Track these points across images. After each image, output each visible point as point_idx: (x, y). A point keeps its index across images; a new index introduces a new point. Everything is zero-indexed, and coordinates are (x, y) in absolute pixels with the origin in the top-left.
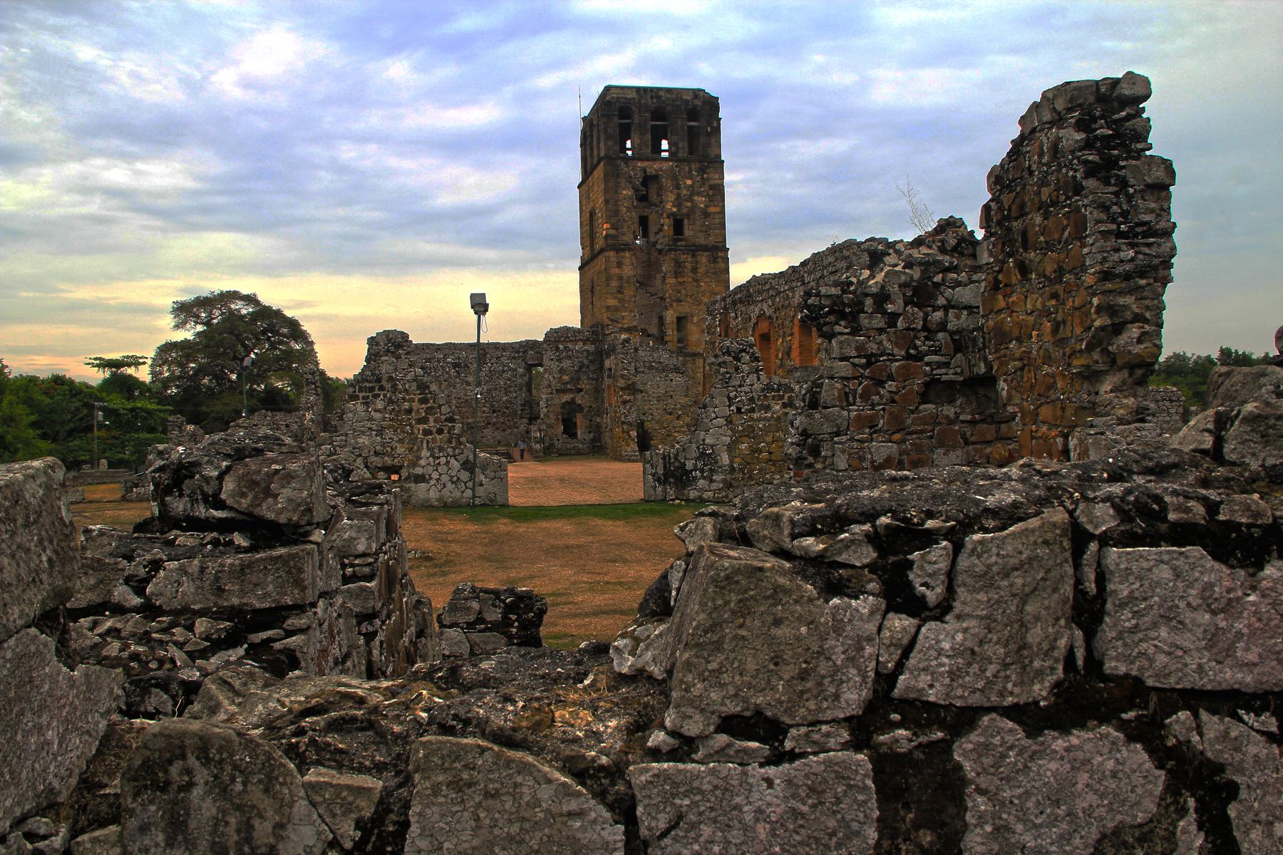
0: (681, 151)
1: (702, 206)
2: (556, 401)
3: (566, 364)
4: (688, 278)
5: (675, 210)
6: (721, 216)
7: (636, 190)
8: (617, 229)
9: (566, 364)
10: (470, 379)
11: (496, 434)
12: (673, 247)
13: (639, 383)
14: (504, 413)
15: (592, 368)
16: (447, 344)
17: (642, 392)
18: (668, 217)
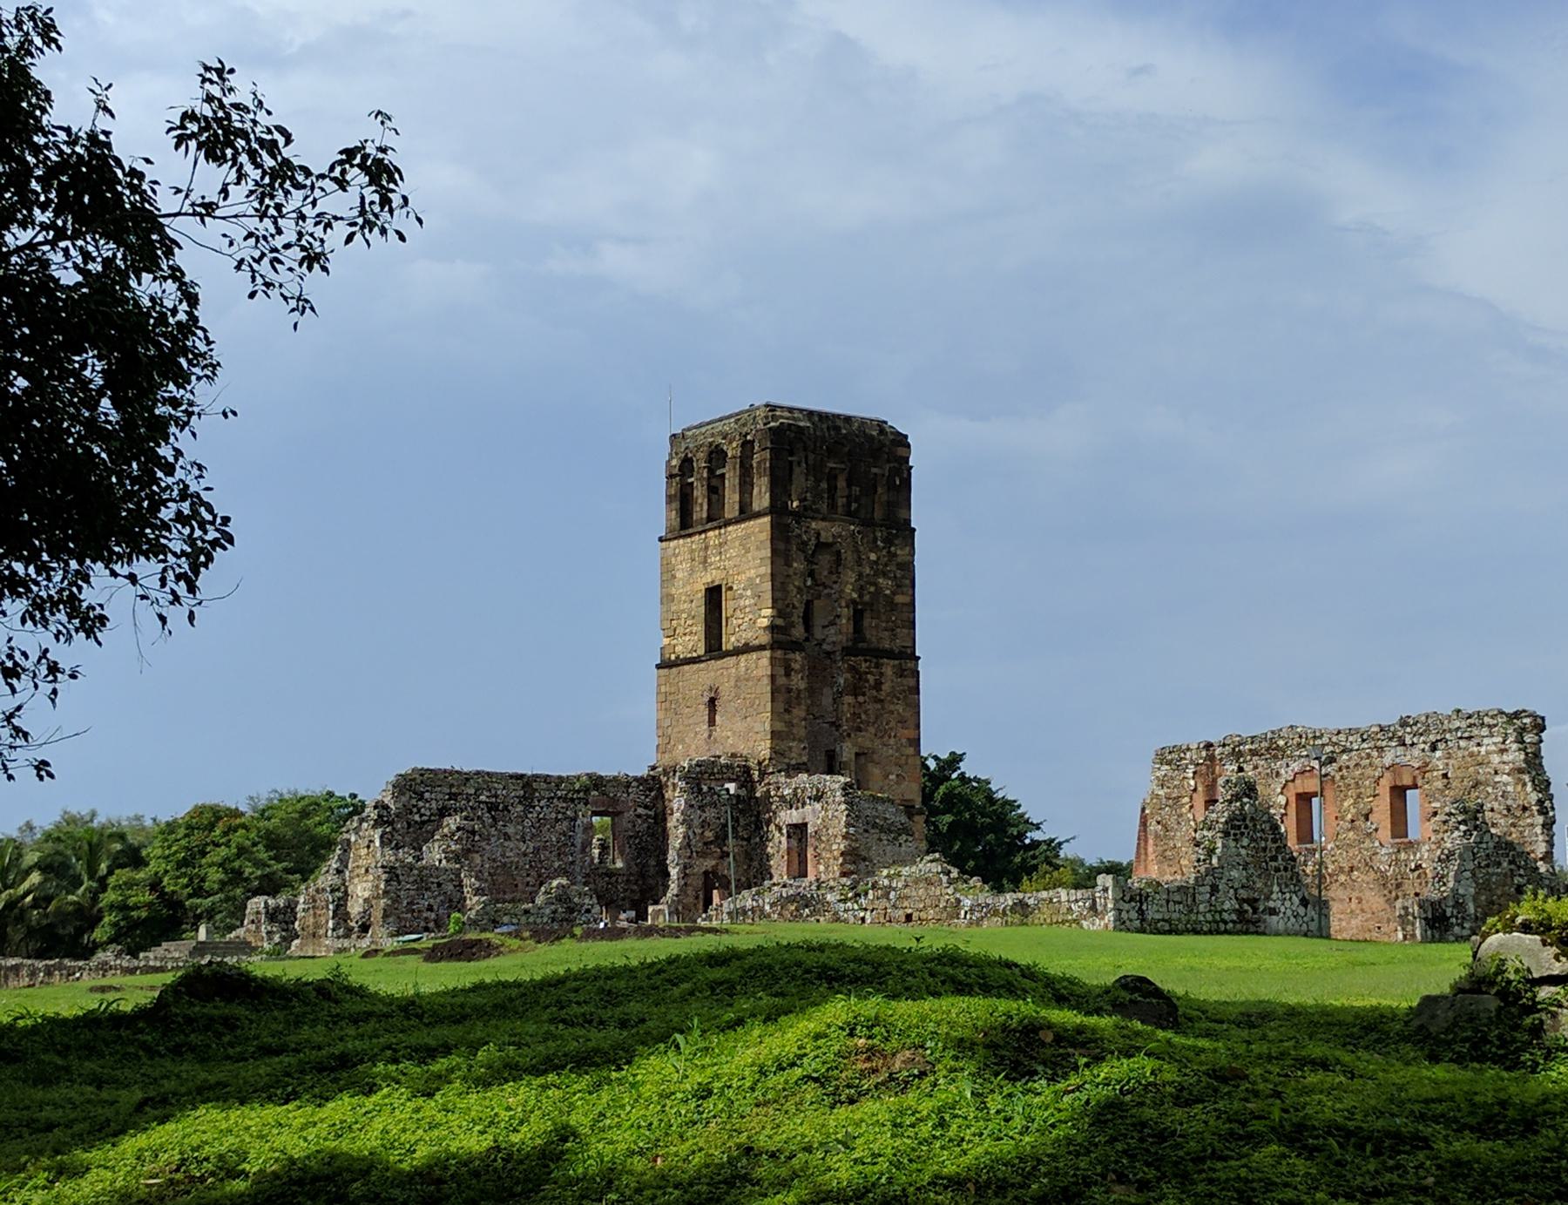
1: (888, 592)
3: (710, 814)
5: (855, 595)
10: (510, 830)
17: (864, 859)
18: (847, 606)
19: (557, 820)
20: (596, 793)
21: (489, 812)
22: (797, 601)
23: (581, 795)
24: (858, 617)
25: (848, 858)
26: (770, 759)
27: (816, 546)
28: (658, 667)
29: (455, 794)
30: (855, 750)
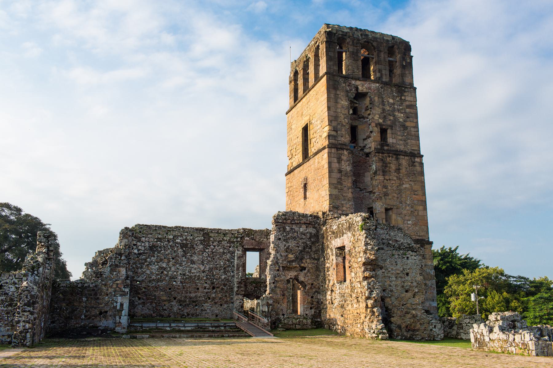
0: (384, 77)
1: (401, 120)
2: (283, 278)
3: (292, 244)
4: (393, 176)
5: (381, 121)
6: (416, 130)
7: (351, 102)
8: (337, 132)
9: (292, 244)
10: (195, 258)
12: (379, 151)
13: (380, 259)
14: (222, 289)
15: (314, 249)
16: (176, 227)
17: (381, 268)
18: (376, 126)
19: (224, 253)
21: (182, 248)
23: (239, 239)
24: (383, 132)
25: (369, 267)
26: (330, 211)
27: (356, 94)
28: (286, 175)
29: (160, 239)
30: (385, 206)
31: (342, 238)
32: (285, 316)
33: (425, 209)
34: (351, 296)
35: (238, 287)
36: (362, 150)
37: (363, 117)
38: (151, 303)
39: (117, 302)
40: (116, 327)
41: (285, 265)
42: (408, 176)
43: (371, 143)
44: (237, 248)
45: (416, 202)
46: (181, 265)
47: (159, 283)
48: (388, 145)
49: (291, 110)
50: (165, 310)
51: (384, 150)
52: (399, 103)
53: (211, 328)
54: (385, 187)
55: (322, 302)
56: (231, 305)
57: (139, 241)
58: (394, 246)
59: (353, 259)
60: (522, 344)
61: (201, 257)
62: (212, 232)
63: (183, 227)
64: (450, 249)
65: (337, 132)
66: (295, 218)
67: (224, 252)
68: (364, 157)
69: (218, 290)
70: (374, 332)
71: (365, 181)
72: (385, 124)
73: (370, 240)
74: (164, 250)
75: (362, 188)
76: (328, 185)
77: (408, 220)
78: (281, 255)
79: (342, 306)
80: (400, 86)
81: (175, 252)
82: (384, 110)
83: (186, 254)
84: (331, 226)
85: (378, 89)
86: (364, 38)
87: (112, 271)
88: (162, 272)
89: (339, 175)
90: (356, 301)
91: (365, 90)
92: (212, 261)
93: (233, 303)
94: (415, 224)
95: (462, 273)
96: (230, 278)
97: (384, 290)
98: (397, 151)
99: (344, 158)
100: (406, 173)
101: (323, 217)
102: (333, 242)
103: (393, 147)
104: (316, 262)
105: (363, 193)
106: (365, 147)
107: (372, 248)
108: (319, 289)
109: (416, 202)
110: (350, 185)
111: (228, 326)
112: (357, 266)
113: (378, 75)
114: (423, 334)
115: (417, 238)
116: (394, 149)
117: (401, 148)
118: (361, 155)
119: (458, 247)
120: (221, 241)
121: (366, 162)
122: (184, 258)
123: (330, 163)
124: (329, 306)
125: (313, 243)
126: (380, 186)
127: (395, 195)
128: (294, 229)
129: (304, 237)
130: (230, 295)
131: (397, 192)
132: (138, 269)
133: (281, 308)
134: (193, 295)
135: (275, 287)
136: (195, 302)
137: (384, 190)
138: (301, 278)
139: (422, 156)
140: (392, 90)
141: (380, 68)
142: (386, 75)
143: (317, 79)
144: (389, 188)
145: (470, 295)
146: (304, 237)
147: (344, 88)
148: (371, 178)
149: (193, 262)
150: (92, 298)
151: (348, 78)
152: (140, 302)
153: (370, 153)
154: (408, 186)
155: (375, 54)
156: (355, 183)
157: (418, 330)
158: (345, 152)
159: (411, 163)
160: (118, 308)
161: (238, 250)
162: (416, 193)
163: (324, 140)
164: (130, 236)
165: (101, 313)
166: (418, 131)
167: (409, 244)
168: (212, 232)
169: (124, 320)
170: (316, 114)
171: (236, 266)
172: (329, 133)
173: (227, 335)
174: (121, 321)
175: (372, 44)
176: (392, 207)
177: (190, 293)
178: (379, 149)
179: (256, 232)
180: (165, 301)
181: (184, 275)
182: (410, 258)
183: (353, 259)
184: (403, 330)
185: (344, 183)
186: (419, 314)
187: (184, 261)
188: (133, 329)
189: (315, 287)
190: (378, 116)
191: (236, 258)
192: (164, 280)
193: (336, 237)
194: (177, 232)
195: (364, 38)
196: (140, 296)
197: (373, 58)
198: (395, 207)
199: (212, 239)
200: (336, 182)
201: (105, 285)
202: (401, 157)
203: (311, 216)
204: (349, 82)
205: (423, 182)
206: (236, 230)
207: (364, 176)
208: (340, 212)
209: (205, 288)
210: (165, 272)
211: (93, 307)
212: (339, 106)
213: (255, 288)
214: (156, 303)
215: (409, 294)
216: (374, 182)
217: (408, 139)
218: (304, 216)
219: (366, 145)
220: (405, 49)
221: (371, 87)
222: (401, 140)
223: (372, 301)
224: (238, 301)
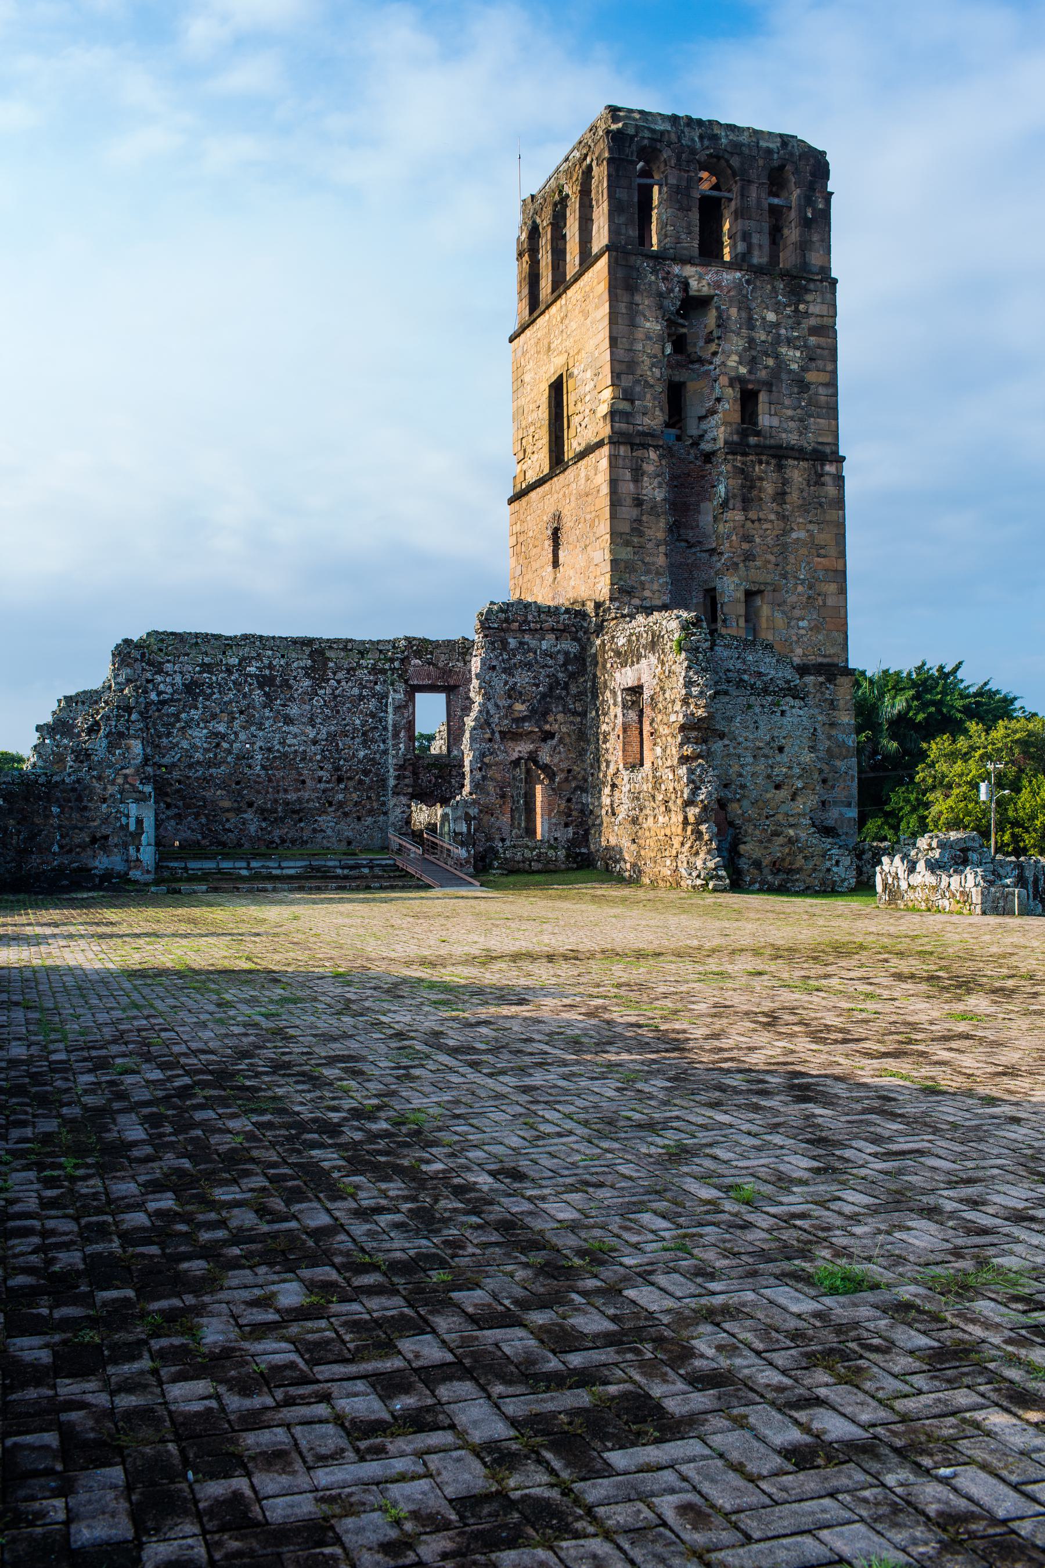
0: (756, 253)
1: (794, 366)
3: (522, 679)
4: (769, 511)
5: (743, 370)
6: (830, 391)
7: (671, 323)
8: (632, 402)
9: (522, 679)
10: (294, 710)
11: (342, 826)
12: (734, 448)
13: (718, 716)
14: (361, 782)
15: (574, 690)
16: (245, 637)
17: (722, 736)
18: (731, 385)
19: (361, 698)
20: (418, 661)
21: (261, 687)
22: (652, 373)
23: (397, 664)
24: (748, 400)
25: (694, 734)
26: (611, 600)
27: (683, 301)
28: (511, 501)
29: (209, 665)
31: (636, 666)
32: (508, 843)
33: (843, 591)
34: (653, 797)
35: (397, 778)
36: (695, 444)
37: (701, 361)
38: (197, 816)
39: (128, 816)
40: (130, 869)
41: (505, 729)
42: (806, 511)
43: (717, 427)
44: (392, 684)
45: (821, 574)
46: (261, 727)
47: (213, 770)
48: (758, 434)
49: (523, 332)
50: (230, 831)
51: (748, 446)
52: (790, 321)
53: (339, 871)
54: (747, 538)
55: (591, 812)
56: (382, 818)
57: (160, 671)
58: (752, 686)
59: (660, 717)
60: (962, 893)
61: (308, 707)
62: (331, 647)
63: (261, 637)
64: (941, 668)
65: (632, 402)
66: (530, 618)
67: (361, 694)
68: (699, 463)
69: (351, 784)
70: (698, 876)
71: (701, 524)
72: (752, 377)
73: (696, 673)
74: (220, 692)
75: (693, 541)
76: (608, 536)
77: (798, 619)
78: (497, 706)
79: (635, 821)
80: (795, 277)
81: (245, 696)
82: (751, 341)
83: (271, 701)
84: (613, 637)
85: (738, 286)
86: (707, 148)
87: (111, 747)
88: (218, 745)
89: (635, 512)
90: (663, 809)
91: (705, 291)
92: (334, 717)
93: (385, 814)
94: (816, 629)
95: (965, 731)
96: (378, 756)
97: (726, 786)
98: (780, 447)
99: (649, 468)
100: (800, 502)
101: (597, 615)
102: (617, 675)
103: (771, 437)
104: (579, 719)
105: (695, 553)
106: (701, 437)
107: (701, 692)
108: (586, 781)
109: (821, 574)
110: (661, 535)
111: (378, 865)
112: (667, 731)
113: (741, 247)
114: (808, 880)
115: (820, 660)
116: (772, 441)
117: (792, 438)
118: (691, 457)
119: (960, 663)
120: (354, 669)
121: (704, 477)
122: (267, 710)
123: (614, 483)
124: (606, 819)
125: (572, 676)
126: (734, 538)
127: (772, 558)
128: (527, 644)
129: (550, 662)
130: (378, 796)
131: (775, 550)
132: (160, 737)
133: (497, 824)
134: (292, 796)
135: (484, 778)
136: (297, 812)
137: (745, 546)
138: (545, 757)
139: (844, 458)
140: (774, 287)
141: (747, 228)
142: (760, 246)
143: (587, 260)
144: (758, 540)
145: (976, 787)
146: (550, 662)
147: (654, 287)
148: (715, 519)
149: (289, 720)
150: (71, 808)
151: (665, 259)
152: (169, 813)
153: (713, 453)
154: (802, 535)
155: (736, 188)
156: (675, 530)
157: (799, 871)
158: (653, 455)
159: (814, 477)
160: (132, 827)
161: (395, 691)
162: (822, 552)
163: (601, 422)
164: (136, 660)
165: (94, 840)
166: (835, 395)
167: (788, 682)
168: (331, 647)
169: (147, 855)
170: (583, 354)
171: (390, 728)
172: (613, 405)
173: (377, 885)
174: (141, 857)
175: (727, 161)
176: (762, 587)
177: (286, 791)
178: (736, 444)
179: (437, 644)
180: (228, 810)
181: (270, 750)
182: (788, 714)
183: (660, 717)
184: (766, 871)
185: (648, 532)
186: (803, 835)
187: (268, 718)
188: (166, 874)
189: (575, 778)
190: (735, 358)
191: (390, 710)
192: (224, 761)
193: (624, 665)
194: (247, 649)
195: (707, 148)
196: (169, 800)
197: (730, 200)
198: (770, 588)
199: (331, 664)
200: (628, 530)
201: (99, 778)
202: (791, 462)
203: (567, 611)
204: (666, 269)
205: (841, 525)
206: (389, 641)
207: (699, 512)
208: (636, 602)
209: (320, 780)
210: (225, 745)
211: (75, 827)
212: (640, 334)
213: (436, 778)
214: (207, 816)
215: (783, 794)
216: (721, 526)
217: (810, 416)
218: (552, 612)
219: (706, 431)
220: (813, 175)
221: (721, 281)
222: (792, 419)
223: (697, 810)
224: (399, 810)
